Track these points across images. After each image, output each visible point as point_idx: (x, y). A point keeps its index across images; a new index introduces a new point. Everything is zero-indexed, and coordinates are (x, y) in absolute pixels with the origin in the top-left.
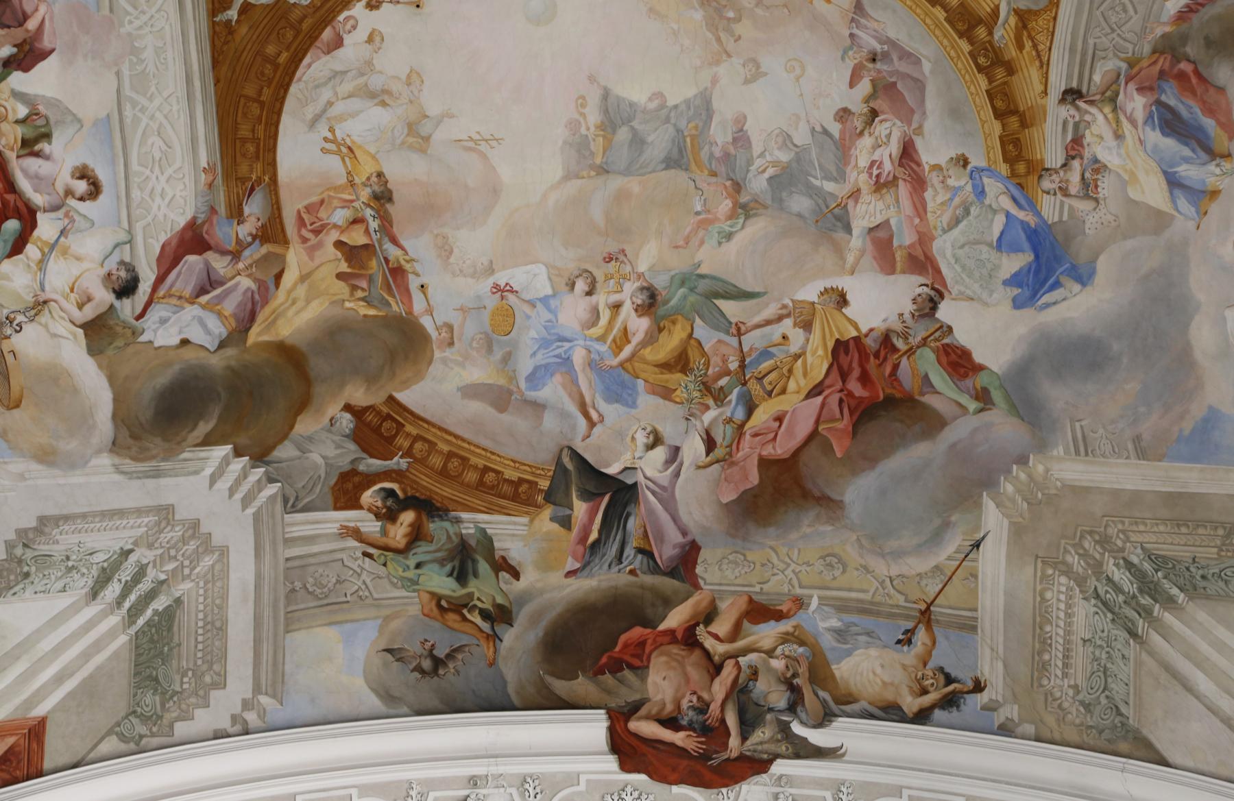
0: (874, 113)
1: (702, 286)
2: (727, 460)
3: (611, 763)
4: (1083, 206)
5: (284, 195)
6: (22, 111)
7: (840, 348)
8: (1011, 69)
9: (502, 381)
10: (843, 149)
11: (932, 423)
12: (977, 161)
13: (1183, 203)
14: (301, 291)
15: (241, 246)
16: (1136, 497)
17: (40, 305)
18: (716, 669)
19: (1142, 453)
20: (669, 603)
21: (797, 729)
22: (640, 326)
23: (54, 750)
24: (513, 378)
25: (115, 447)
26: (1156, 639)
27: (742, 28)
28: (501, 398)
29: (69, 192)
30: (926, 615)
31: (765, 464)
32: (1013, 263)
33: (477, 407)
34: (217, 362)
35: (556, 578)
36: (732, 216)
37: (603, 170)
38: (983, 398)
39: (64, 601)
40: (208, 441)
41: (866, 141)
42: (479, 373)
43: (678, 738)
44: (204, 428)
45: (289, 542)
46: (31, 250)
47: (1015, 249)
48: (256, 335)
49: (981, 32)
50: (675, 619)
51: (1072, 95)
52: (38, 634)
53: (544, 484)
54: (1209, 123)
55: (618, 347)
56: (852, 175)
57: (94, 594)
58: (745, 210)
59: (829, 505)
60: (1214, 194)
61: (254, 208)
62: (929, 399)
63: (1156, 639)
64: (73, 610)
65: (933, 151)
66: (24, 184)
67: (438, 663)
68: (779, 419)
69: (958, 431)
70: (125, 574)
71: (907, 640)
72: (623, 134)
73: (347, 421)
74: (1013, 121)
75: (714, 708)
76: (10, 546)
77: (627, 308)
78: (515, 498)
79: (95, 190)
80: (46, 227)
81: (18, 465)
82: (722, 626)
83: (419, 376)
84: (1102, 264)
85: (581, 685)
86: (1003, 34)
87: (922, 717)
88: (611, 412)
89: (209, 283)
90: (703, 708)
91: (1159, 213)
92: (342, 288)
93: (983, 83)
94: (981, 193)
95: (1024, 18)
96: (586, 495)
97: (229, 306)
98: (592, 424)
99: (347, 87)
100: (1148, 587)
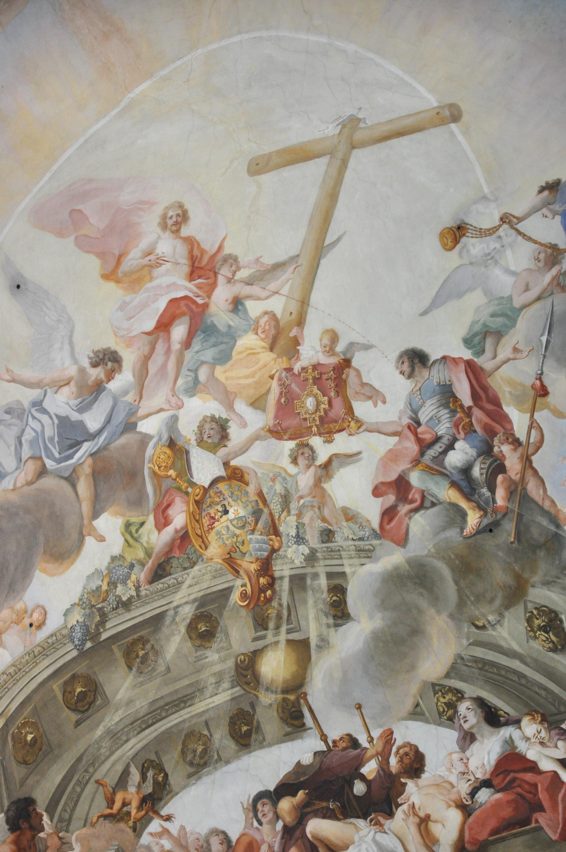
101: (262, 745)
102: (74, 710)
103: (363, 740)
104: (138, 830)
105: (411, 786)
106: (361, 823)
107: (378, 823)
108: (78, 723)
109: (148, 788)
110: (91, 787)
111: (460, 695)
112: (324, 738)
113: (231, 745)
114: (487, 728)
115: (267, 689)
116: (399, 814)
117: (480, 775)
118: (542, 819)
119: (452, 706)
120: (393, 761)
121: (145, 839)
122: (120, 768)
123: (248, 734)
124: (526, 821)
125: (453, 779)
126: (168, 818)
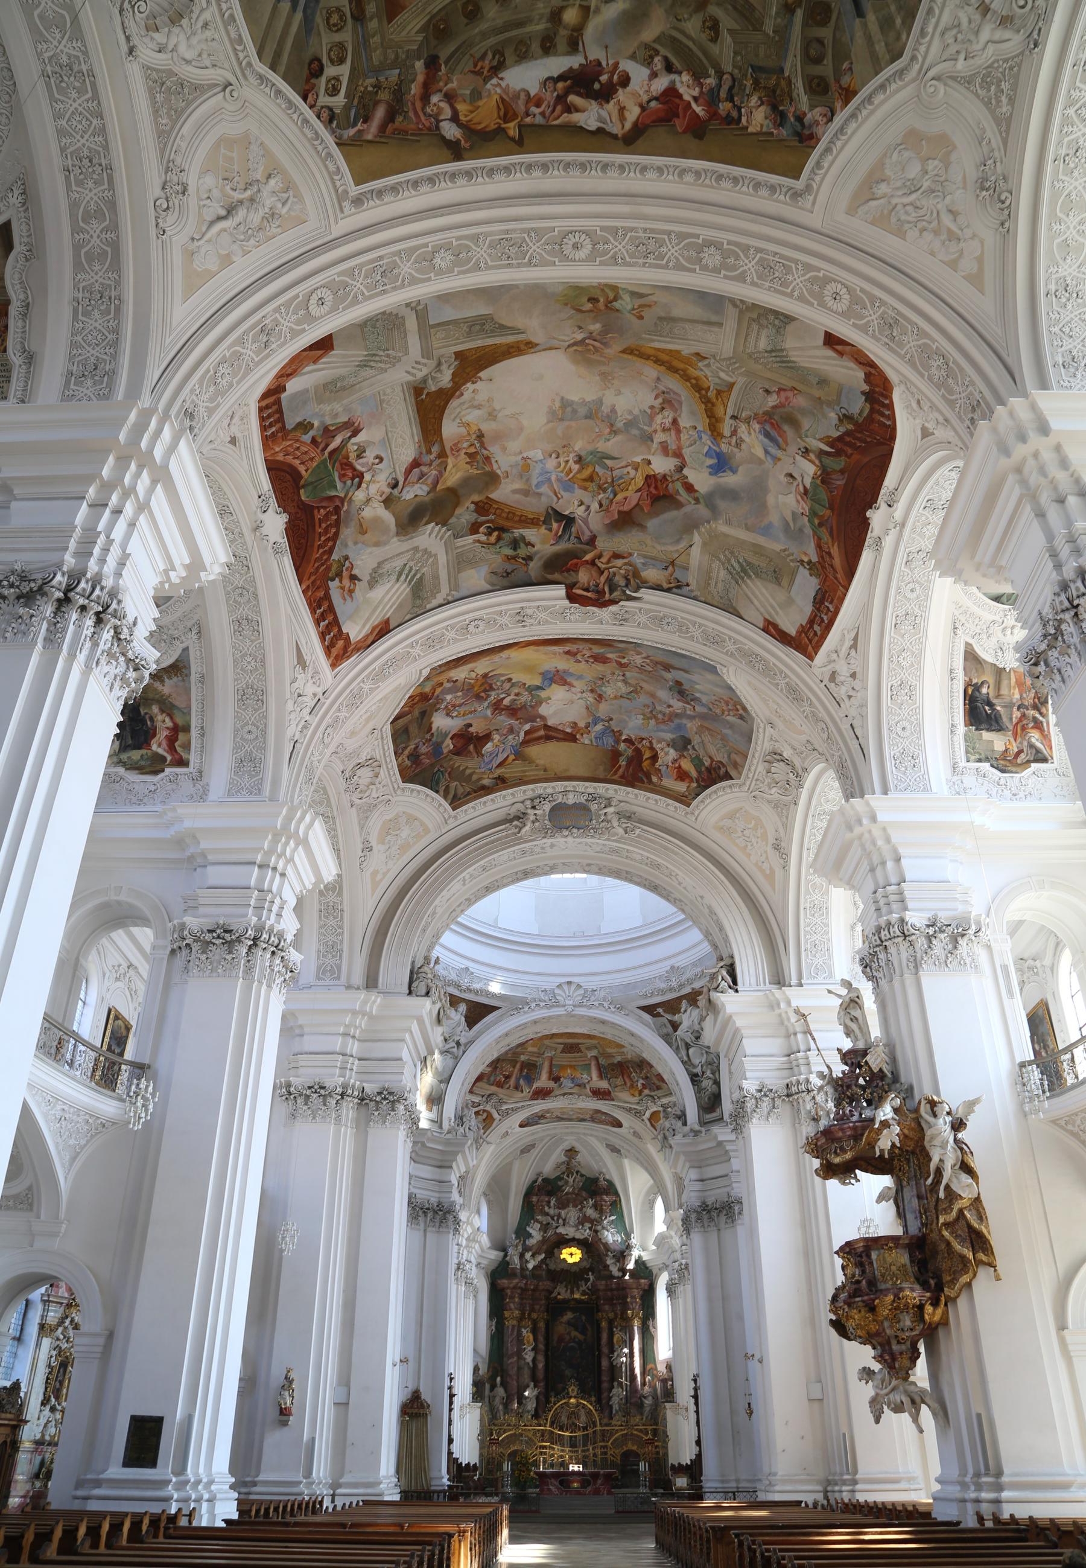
0: (663, 408)
1: (598, 455)
2: (607, 510)
3: (567, 602)
4: (736, 450)
5: (445, 442)
6: (356, 447)
7: (648, 477)
8: (713, 405)
9: (526, 487)
10: (652, 418)
11: (679, 505)
12: (700, 428)
13: (769, 458)
14: (454, 471)
15: (432, 462)
16: (744, 542)
17: (368, 500)
18: (602, 573)
19: (748, 528)
20: (586, 553)
21: (628, 592)
22: (576, 467)
23: (392, 625)
24: (530, 486)
25: (398, 534)
26: (744, 586)
27: (615, 382)
28: (526, 493)
29: (373, 464)
30: (672, 563)
31: (619, 512)
32: (710, 461)
33: (517, 496)
34: (427, 499)
35: (547, 546)
36: (610, 434)
37: (562, 420)
38: (697, 500)
39: (389, 585)
40: (427, 523)
41: (660, 416)
42: (517, 485)
43: (589, 594)
44: (425, 520)
45: (456, 548)
46: (364, 485)
47: (711, 457)
48: (439, 487)
49: (703, 392)
50: (588, 557)
51: (734, 417)
52: (383, 597)
53: (542, 519)
54: (780, 439)
55: (568, 474)
56: (654, 426)
57: (398, 580)
58: (615, 432)
59: (642, 527)
60: (779, 459)
61: (435, 449)
62: (678, 497)
63: (744, 586)
64: (393, 586)
65: (684, 422)
66: (359, 467)
67: (508, 574)
68: (626, 499)
69: (687, 509)
70: (406, 572)
71: (666, 568)
72: (569, 409)
73: (472, 507)
74: (713, 420)
75: (601, 585)
76: (371, 575)
77: (571, 461)
78: (532, 523)
79: (381, 460)
80: (367, 477)
81: (370, 550)
82: (604, 560)
83: (497, 488)
84: (740, 469)
85: (556, 576)
86: (711, 394)
87: (668, 590)
88: (565, 495)
89: (422, 475)
90: (597, 585)
91: (760, 459)
92: (468, 466)
93: (703, 406)
94: (701, 438)
95: (719, 393)
96: (557, 521)
97: (429, 481)
98: (559, 499)
99: (466, 406)
100: (744, 570)
101: (555, 54)
102: (466, 17)
103: (604, 64)
104: (486, 80)
105: (620, 91)
106: (593, 102)
107: (601, 104)
108: (467, 25)
109: (495, 63)
110: (467, 56)
111: (657, 53)
112: (586, 58)
113: (540, 51)
114: (664, 72)
115: (565, 27)
116: (612, 103)
117: (654, 94)
118: (677, 122)
119: (652, 57)
120: (616, 77)
121: (488, 86)
122: (483, 50)
123: (550, 48)
124: (670, 121)
125: (641, 93)
126: (502, 79)
